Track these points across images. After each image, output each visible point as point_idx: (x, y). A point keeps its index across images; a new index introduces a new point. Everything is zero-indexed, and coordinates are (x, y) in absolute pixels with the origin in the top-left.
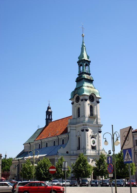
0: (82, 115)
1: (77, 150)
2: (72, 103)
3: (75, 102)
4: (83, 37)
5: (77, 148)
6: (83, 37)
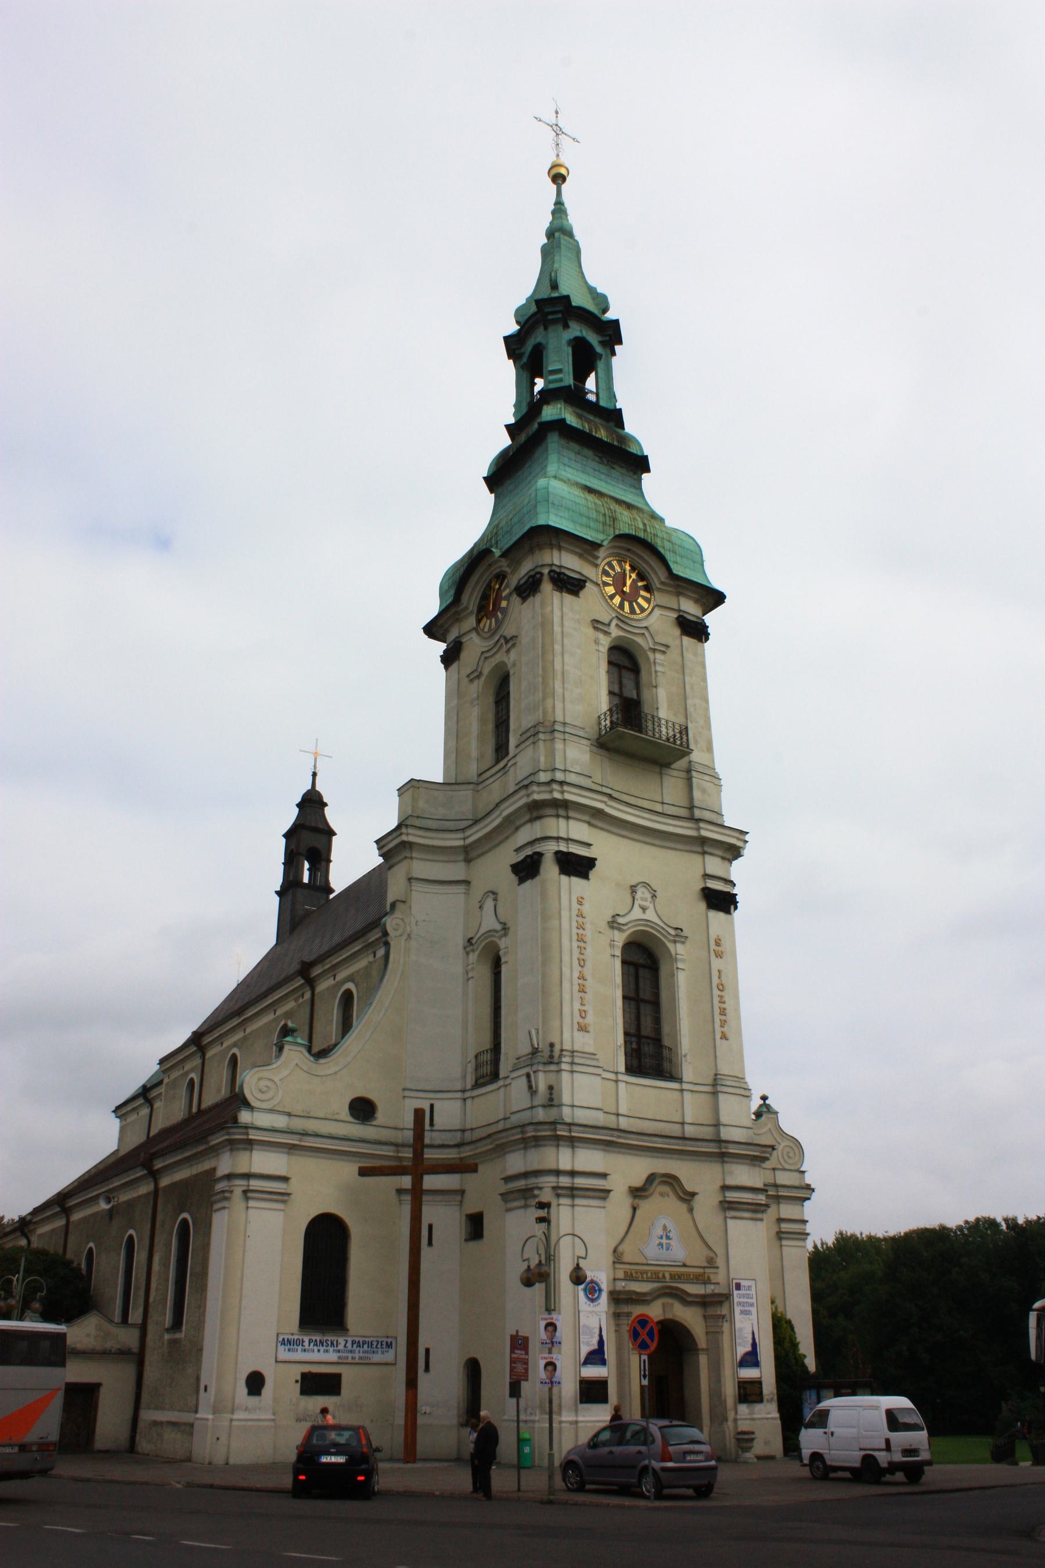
0: (527, 721)
1: (470, 1082)
2: (448, 659)
3: (474, 635)
4: (558, 179)
5: (471, 1068)
6: (558, 179)
